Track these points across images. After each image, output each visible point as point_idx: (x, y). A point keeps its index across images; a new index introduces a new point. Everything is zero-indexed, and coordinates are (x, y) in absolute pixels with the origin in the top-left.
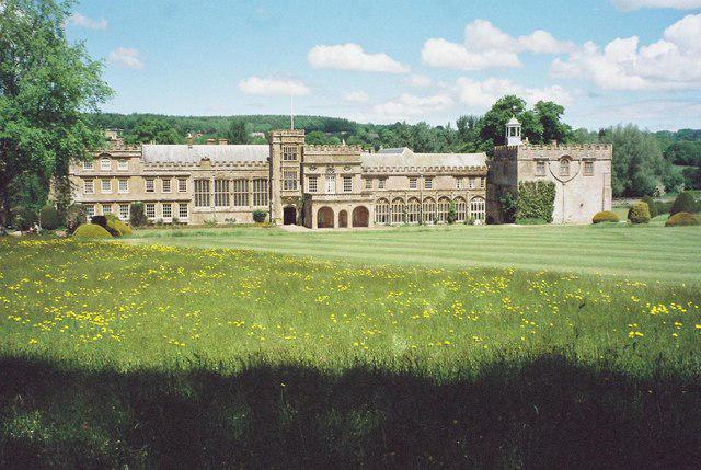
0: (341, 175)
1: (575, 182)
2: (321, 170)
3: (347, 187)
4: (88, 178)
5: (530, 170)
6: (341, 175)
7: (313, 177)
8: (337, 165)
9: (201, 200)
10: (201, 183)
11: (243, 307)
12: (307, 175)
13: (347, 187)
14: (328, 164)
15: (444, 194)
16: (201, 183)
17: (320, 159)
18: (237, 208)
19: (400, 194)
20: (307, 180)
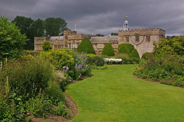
0: (76, 43)
1: (142, 45)
2: (72, 42)
4: (37, 45)
5: (123, 40)
6: (76, 43)
7: (70, 44)
8: (76, 40)
11: (110, 83)
14: (73, 40)
17: (71, 38)
20: (68, 45)
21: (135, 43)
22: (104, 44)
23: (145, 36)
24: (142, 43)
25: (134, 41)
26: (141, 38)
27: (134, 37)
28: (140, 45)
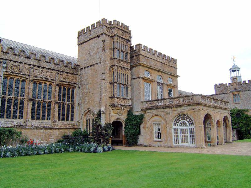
18: (36, 122)
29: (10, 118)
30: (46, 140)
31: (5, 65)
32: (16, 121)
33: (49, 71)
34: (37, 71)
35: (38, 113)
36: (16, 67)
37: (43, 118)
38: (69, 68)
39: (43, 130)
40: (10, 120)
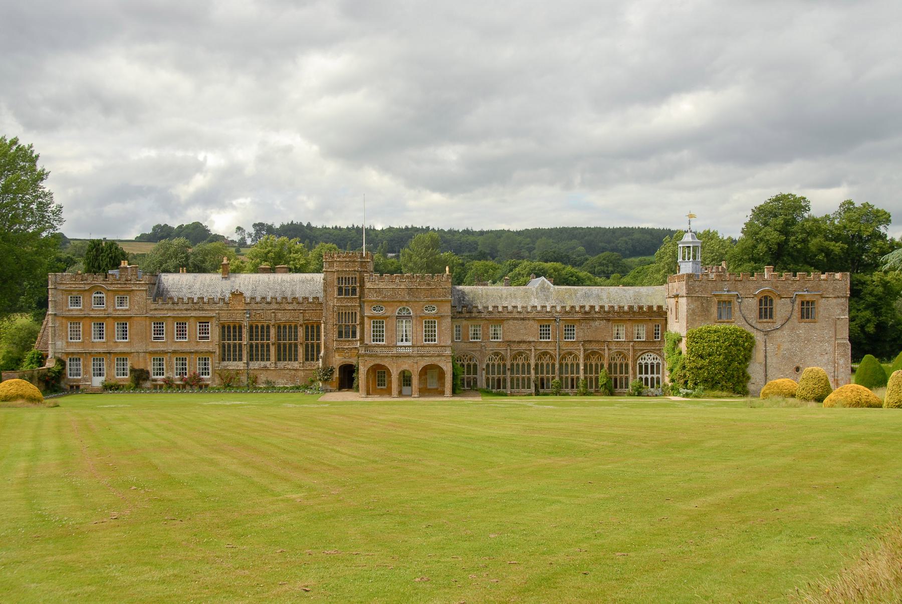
3: (430, 337)
7: (378, 322)
9: (228, 353)
10: (230, 331)
12: (369, 317)
13: (430, 337)
15: (595, 347)
16: (230, 331)
18: (281, 364)
19: (524, 347)
21: (759, 326)
22: (534, 319)
23: (798, 301)
24: (786, 326)
25: (753, 315)
26: (781, 308)
27: (753, 303)
28: (779, 333)
29: (258, 360)
30: (290, 380)
31: (248, 315)
32: (263, 363)
33: (292, 311)
34: (280, 314)
35: (285, 355)
36: (258, 315)
37: (290, 360)
38: (315, 304)
39: (287, 371)
40: (258, 362)
